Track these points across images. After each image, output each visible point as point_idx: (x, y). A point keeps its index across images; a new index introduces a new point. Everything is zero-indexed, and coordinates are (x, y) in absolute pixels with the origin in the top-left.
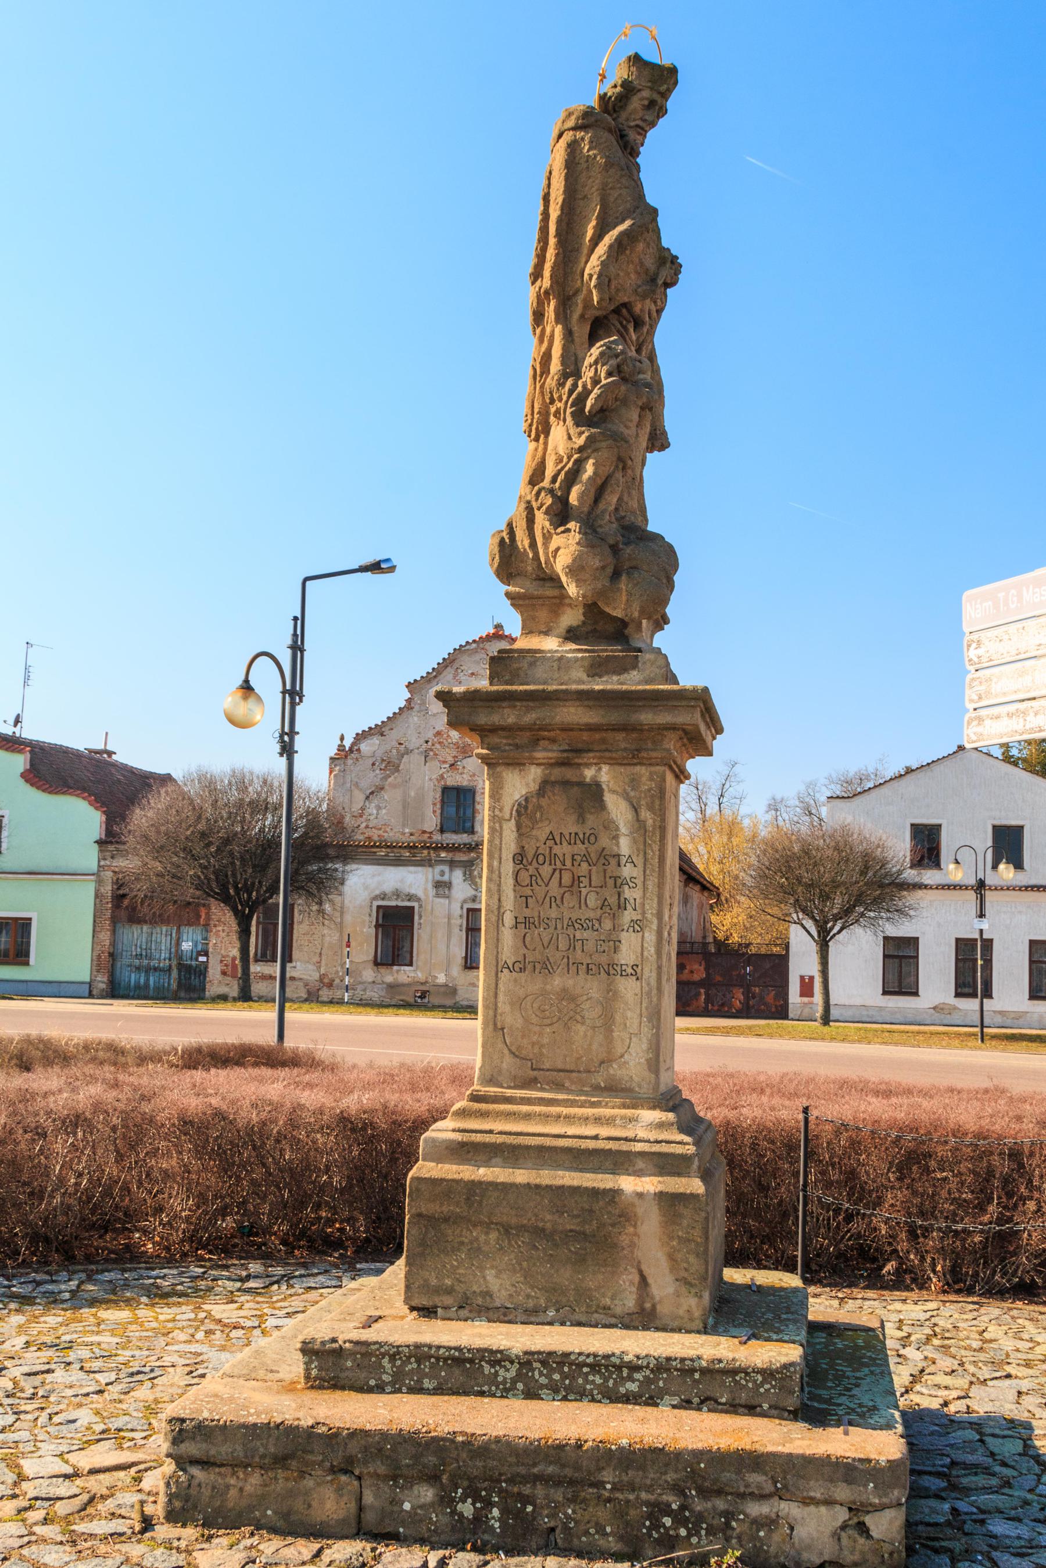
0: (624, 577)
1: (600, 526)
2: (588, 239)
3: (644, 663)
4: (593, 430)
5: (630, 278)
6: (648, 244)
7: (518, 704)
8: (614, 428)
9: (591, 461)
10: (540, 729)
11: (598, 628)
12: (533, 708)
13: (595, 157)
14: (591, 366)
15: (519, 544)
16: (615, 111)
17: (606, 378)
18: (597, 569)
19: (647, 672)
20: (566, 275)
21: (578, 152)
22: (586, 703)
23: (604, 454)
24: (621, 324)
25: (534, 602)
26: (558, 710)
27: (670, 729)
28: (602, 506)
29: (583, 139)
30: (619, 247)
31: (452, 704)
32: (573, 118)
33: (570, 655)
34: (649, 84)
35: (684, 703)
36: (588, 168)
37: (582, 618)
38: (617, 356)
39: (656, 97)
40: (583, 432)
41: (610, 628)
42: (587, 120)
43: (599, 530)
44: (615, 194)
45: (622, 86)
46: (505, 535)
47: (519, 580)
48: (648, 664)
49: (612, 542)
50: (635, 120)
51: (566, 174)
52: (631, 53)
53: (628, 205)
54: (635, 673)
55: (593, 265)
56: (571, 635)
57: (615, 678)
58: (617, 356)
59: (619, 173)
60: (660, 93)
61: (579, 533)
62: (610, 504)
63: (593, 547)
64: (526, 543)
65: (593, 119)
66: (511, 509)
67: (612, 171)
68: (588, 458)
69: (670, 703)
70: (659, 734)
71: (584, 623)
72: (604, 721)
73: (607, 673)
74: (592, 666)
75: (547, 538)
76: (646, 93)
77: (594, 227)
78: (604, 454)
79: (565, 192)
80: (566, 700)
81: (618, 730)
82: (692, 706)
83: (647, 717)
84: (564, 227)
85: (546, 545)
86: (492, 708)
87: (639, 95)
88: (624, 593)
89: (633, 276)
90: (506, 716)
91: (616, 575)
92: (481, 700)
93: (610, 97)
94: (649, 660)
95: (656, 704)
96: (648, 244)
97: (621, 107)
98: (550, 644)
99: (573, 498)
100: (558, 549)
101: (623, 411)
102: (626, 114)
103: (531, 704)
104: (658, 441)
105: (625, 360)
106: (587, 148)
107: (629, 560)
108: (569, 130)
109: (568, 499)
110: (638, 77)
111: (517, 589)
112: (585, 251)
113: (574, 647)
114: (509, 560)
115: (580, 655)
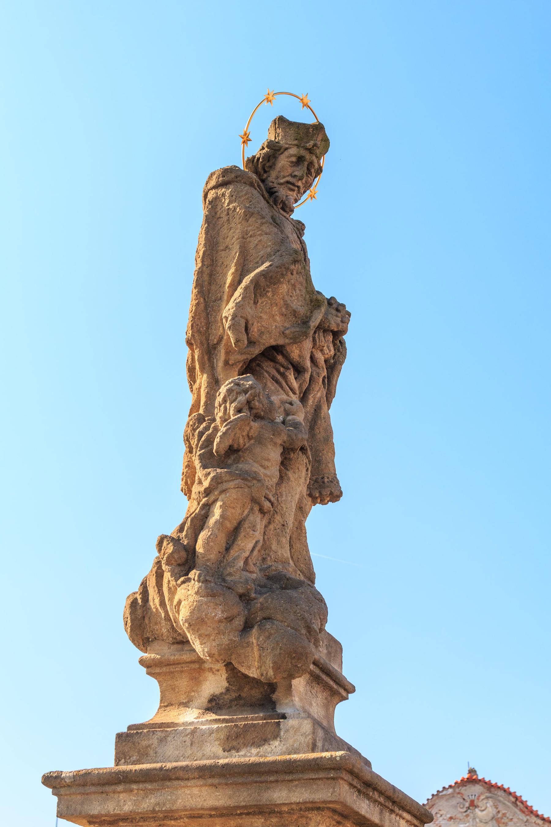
0: (255, 631)
1: (230, 574)
2: (227, 285)
3: (287, 731)
4: (219, 470)
5: (275, 321)
6: (294, 286)
7: (134, 786)
8: (246, 467)
9: (219, 504)
10: (166, 818)
11: (243, 695)
12: (152, 791)
13: (235, 209)
14: (220, 406)
15: (151, 603)
16: (265, 172)
17: (234, 415)
18: (220, 621)
19: (291, 741)
20: (208, 325)
21: (219, 207)
22: (210, 781)
23: (233, 494)
24: (278, 371)
25: (172, 669)
26: (180, 792)
27: (312, 809)
28: (233, 553)
29: (223, 195)
30: (258, 289)
31: (62, 791)
32: (214, 177)
33: (204, 727)
34: (296, 142)
35: (321, 775)
36: (228, 220)
37: (226, 684)
38: (246, 392)
39: (303, 152)
40: (209, 474)
41: (256, 694)
42: (228, 177)
43: (229, 578)
44: (254, 241)
45: (268, 147)
46: (139, 597)
47: (156, 645)
48: (292, 732)
49: (241, 591)
50: (284, 177)
51: (207, 228)
52: (276, 116)
53: (269, 250)
54: (277, 743)
55: (228, 310)
56: (214, 705)
57: (254, 751)
58: (246, 392)
59: (259, 221)
60: (307, 149)
61: (199, 581)
62: (243, 550)
63: (213, 595)
64: (157, 601)
65: (233, 175)
66: (145, 568)
67: (252, 220)
68: (215, 501)
69: (306, 776)
70: (302, 817)
71: (228, 690)
72: (231, 803)
73: (245, 745)
74: (228, 738)
75: (172, 592)
76: (293, 151)
77: (233, 273)
78: (233, 494)
79: (205, 245)
80: (188, 779)
81: (254, 814)
82: (333, 778)
83: (280, 795)
84: (206, 277)
85: (171, 599)
86: (107, 793)
87: (286, 153)
88: (256, 649)
89: (278, 318)
90: (122, 803)
91: (247, 627)
92: (93, 785)
93: (258, 159)
94: (292, 727)
95: (290, 777)
96: (294, 286)
97: (270, 167)
98: (189, 716)
99: (200, 548)
100: (179, 602)
101: (258, 450)
102: (278, 173)
103: (149, 786)
104: (325, 488)
105: (254, 396)
106: (227, 201)
107: (262, 609)
108: (211, 189)
109: (195, 549)
110: (284, 137)
111: (153, 655)
112: (225, 297)
113: (214, 717)
114: (142, 622)
115: (215, 726)
